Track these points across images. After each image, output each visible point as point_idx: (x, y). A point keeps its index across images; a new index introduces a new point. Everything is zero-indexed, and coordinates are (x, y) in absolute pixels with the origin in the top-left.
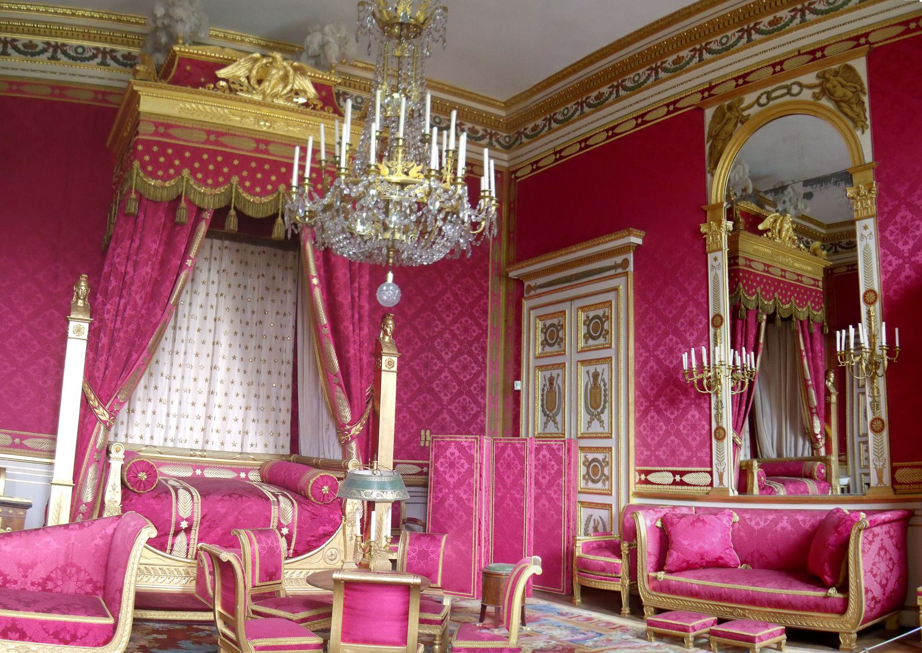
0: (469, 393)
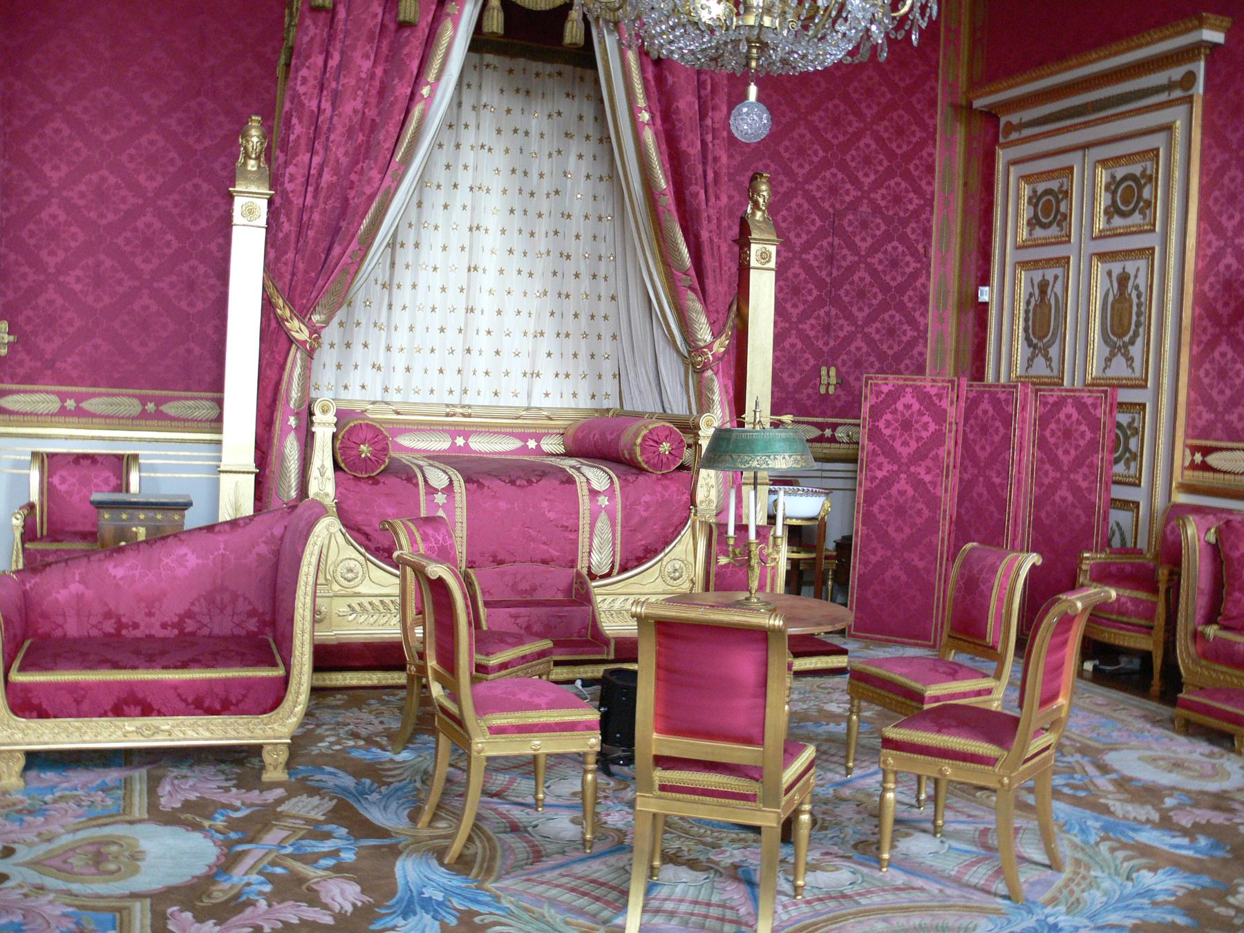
0: (901, 307)
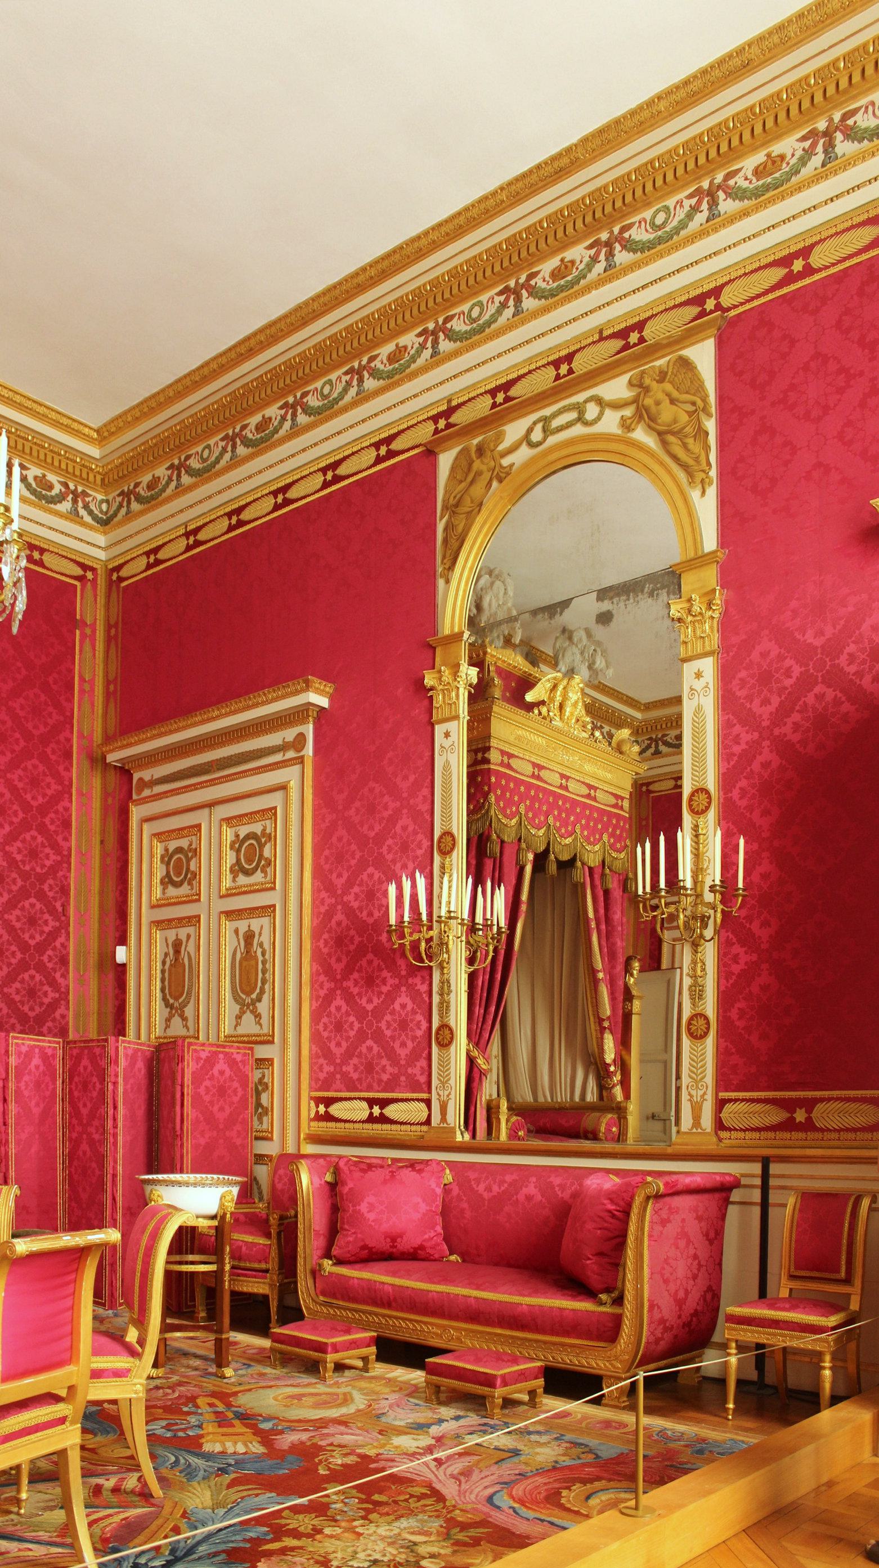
0: (40, 967)
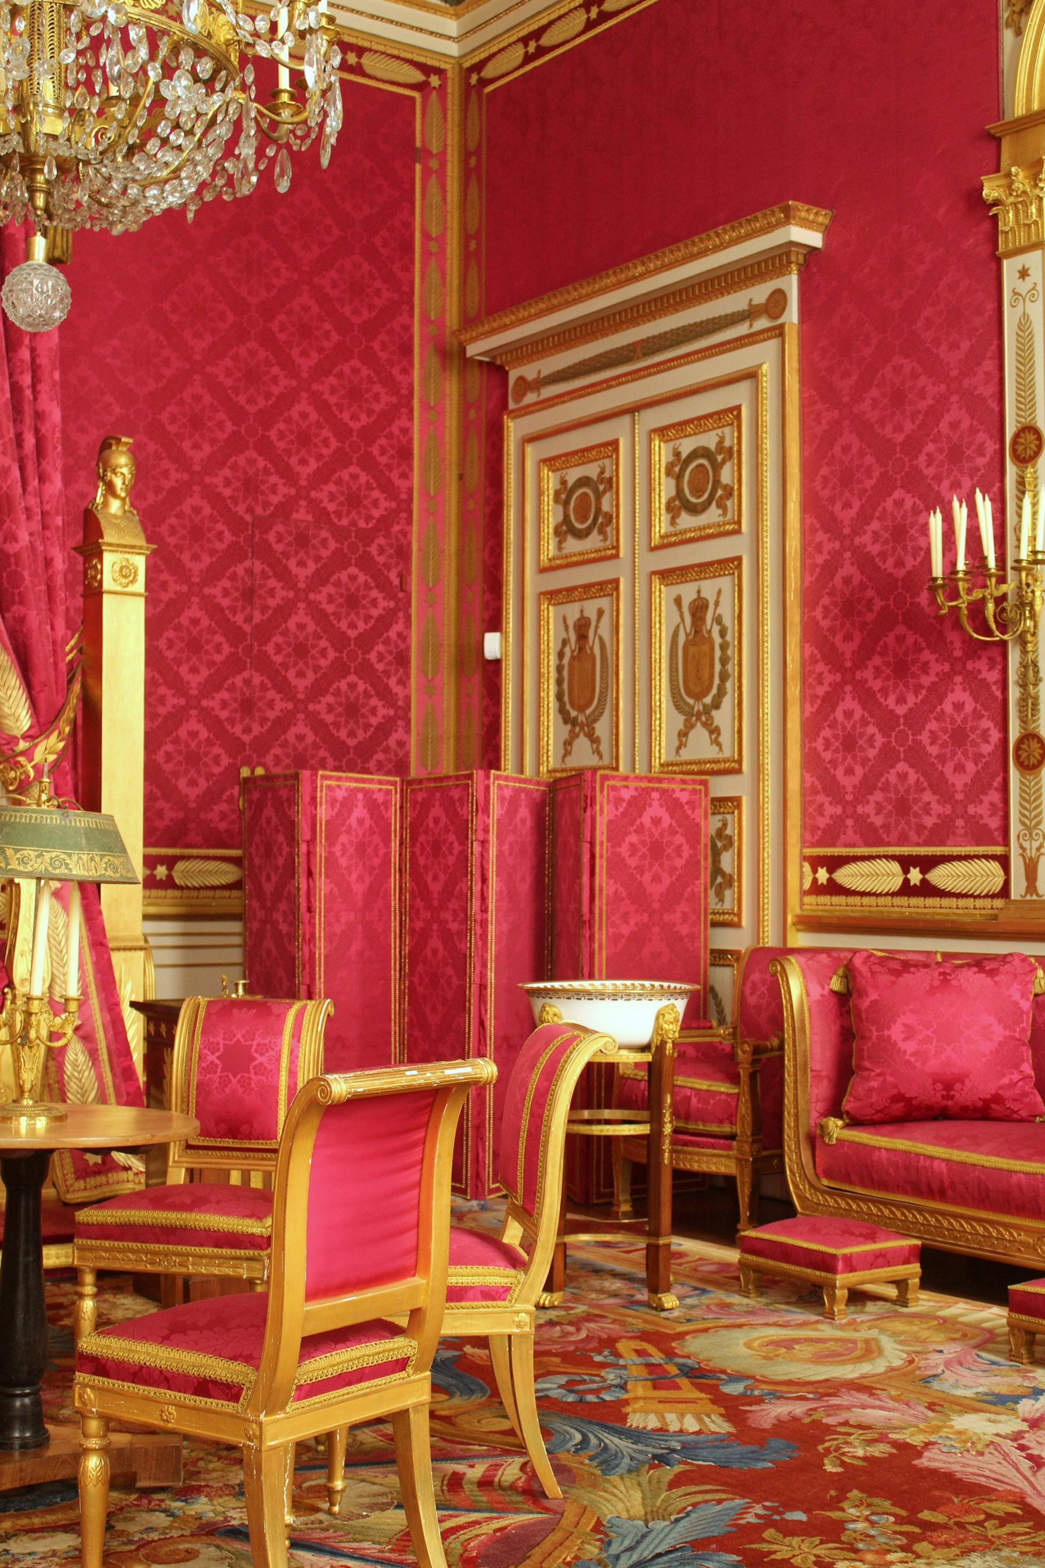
0: (365, 670)
